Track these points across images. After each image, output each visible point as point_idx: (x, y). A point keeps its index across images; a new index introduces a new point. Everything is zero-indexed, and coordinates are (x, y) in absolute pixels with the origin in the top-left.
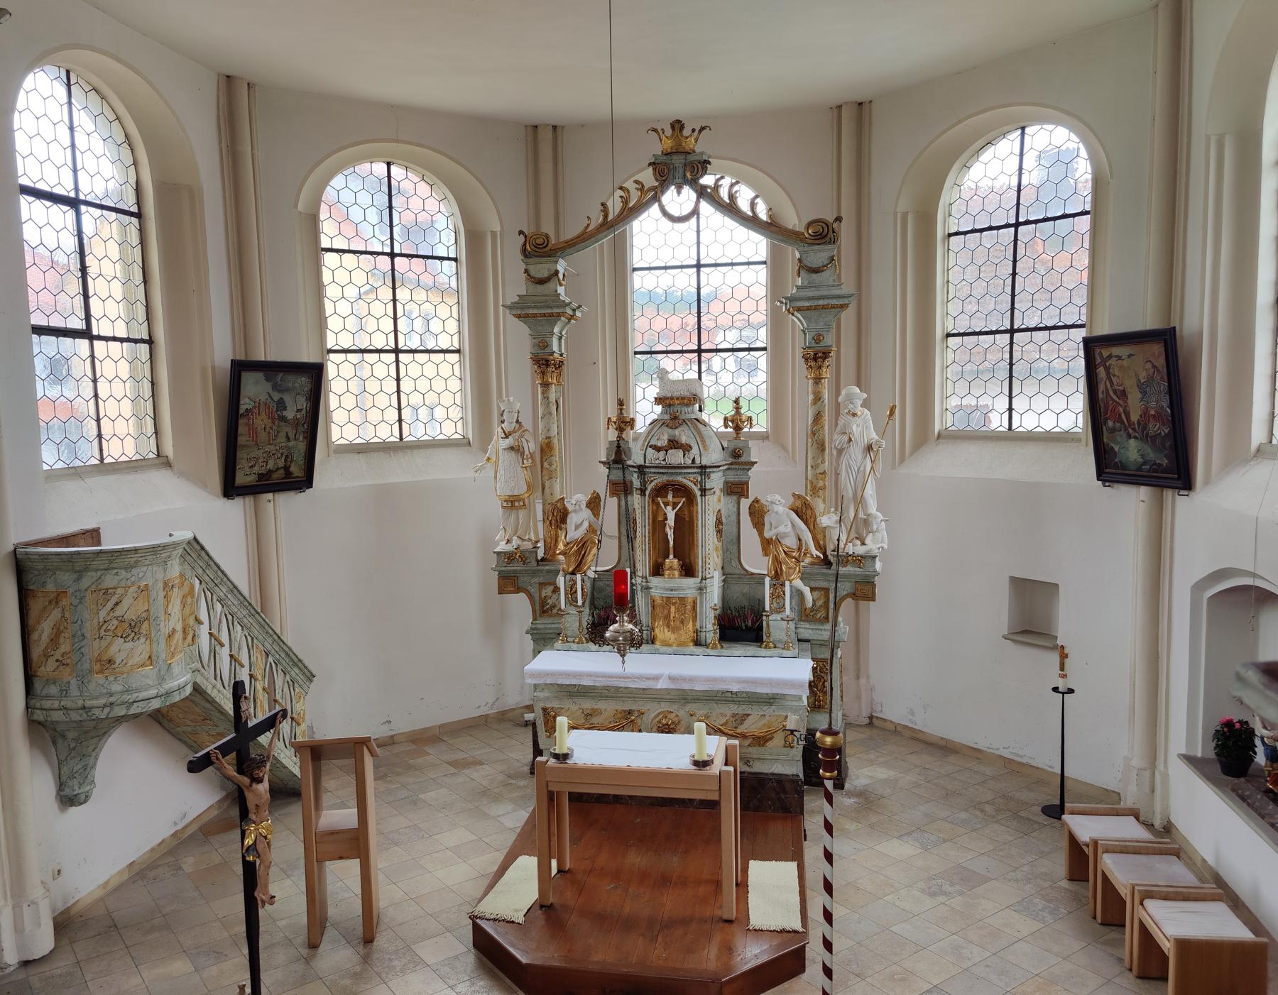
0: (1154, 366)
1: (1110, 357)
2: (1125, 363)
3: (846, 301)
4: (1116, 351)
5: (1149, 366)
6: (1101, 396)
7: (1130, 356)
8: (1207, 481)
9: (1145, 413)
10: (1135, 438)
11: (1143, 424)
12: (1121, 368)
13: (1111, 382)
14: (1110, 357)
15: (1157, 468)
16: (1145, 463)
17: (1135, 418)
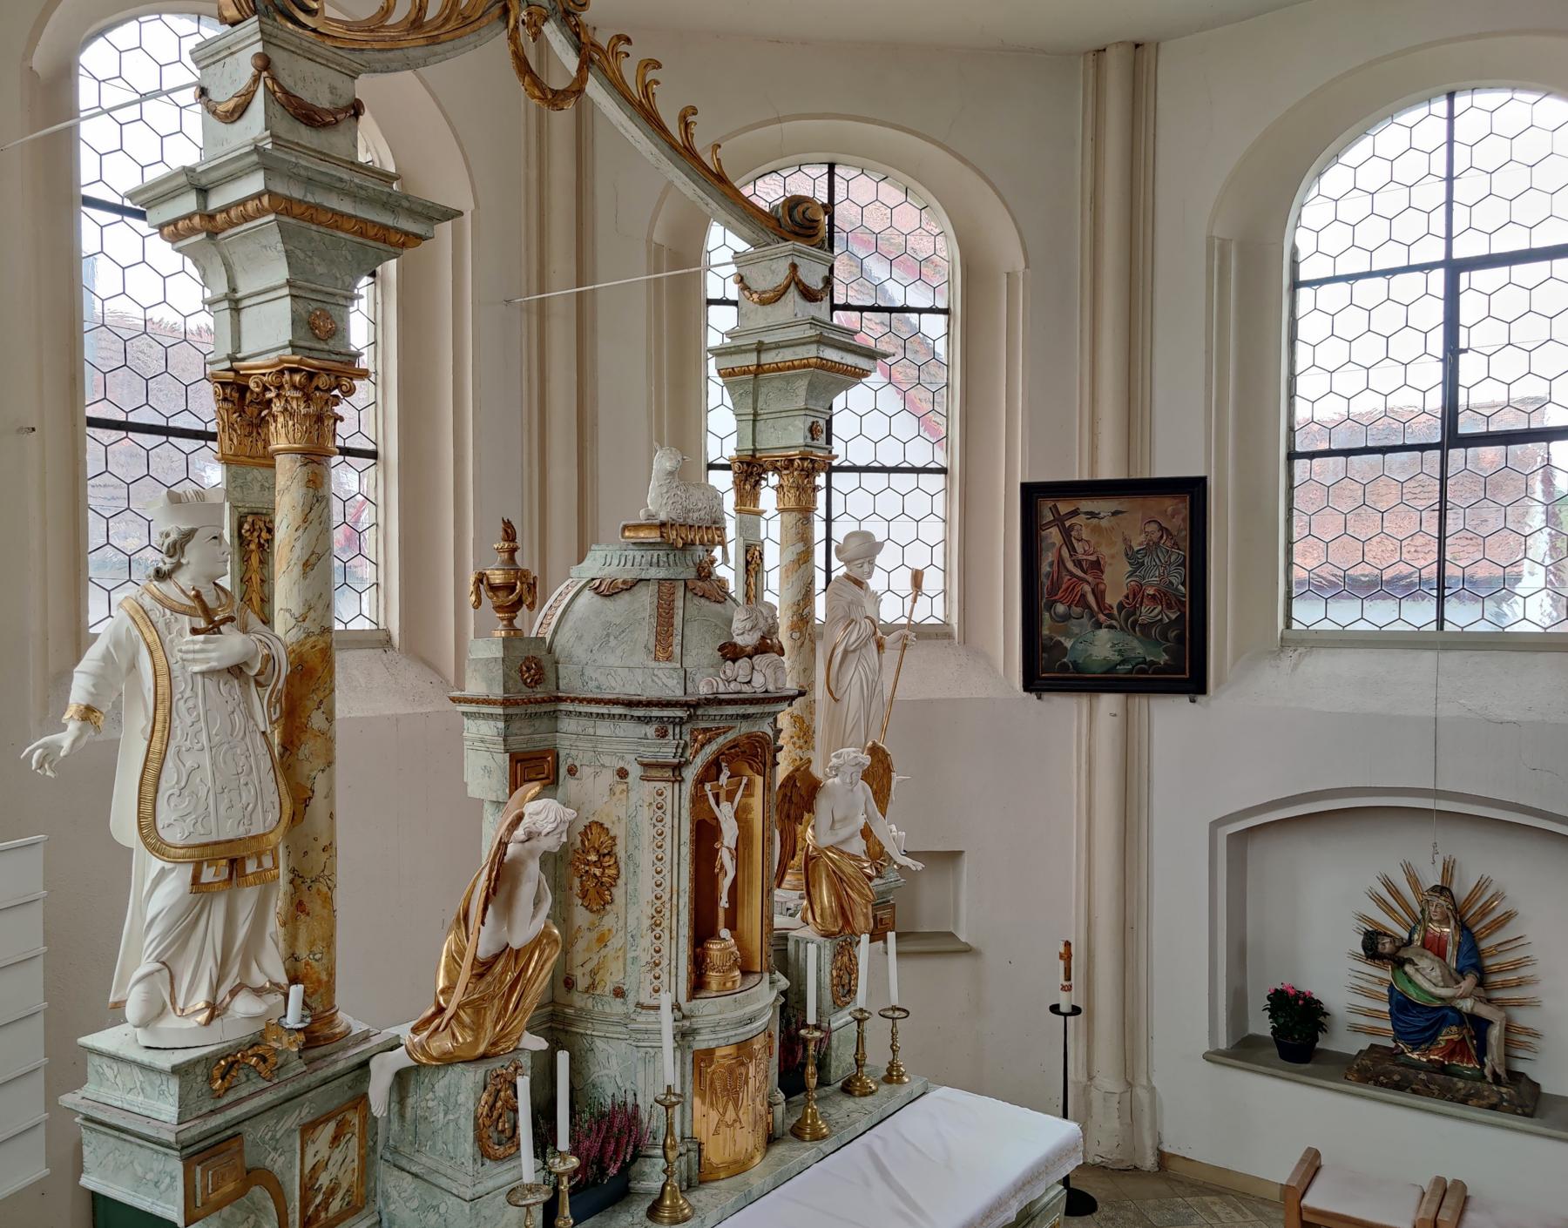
0: (1162, 528)
1: (1075, 513)
2: (1104, 523)
3: (863, 363)
4: (1086, 505)
5: (1153, 527)
6: (1045, 568)
7: (1115, 514)
8: (1217, 685)
9: (1136, 594)
10: (1110, 627)
11: (1129, 609)
12: (1097, 530)
13: (1072, 550)
14: (1075, 513)
15: (1146, 666)
16: (1123, 662)
17: (1112, 599)
